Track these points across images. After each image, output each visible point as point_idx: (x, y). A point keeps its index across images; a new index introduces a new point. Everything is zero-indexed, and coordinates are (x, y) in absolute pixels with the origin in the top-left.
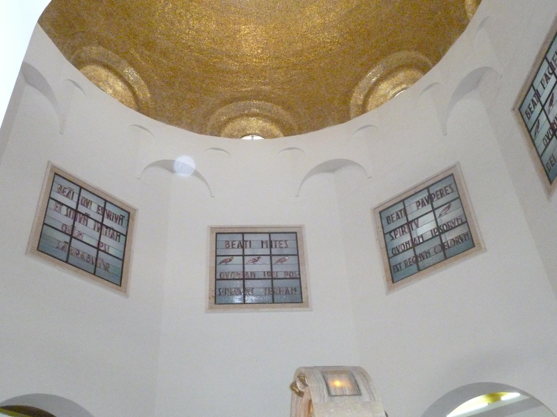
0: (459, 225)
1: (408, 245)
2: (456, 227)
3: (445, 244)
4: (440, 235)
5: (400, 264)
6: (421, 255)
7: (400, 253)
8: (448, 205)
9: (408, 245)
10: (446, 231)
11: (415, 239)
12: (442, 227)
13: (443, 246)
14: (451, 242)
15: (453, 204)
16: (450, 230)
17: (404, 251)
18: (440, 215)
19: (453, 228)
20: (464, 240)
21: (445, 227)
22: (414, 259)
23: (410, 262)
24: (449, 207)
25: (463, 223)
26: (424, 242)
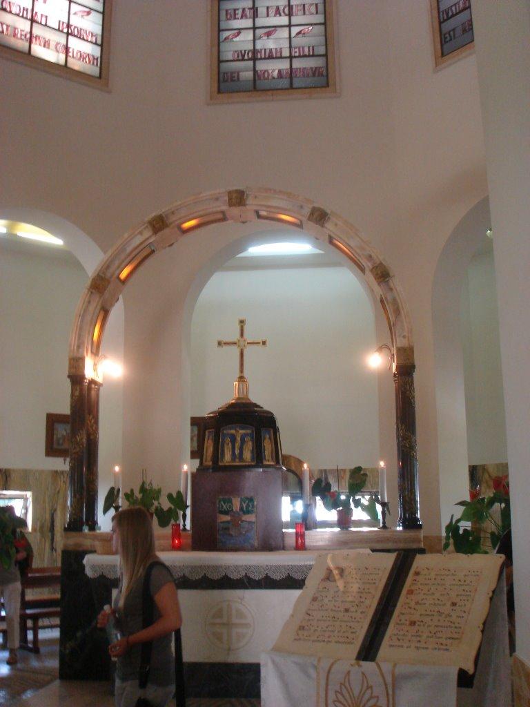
0: (91, 42)
1: (25, 12)
2: (87, 41)
3: (71, 50)
4: (68, 34)
5: (8, 26)
6: (37, 37)
7: (10, 12)
8: (90, 10)
9: (25, 12)
10: (75, 36)
11: (36, 13)
12: (72, 28)
13: (67, 49)
14: (77, 53)
15: (93, 12)
16: (80, 38)
17: (18, 15)
18: (75, 14)
19: (83, 39)
20: (92, 63)
21: (76, 29)
22: (28, 36)
23: (21, 35)
24: (88, 13)
25: (96, 44)
26: (46, 25)
